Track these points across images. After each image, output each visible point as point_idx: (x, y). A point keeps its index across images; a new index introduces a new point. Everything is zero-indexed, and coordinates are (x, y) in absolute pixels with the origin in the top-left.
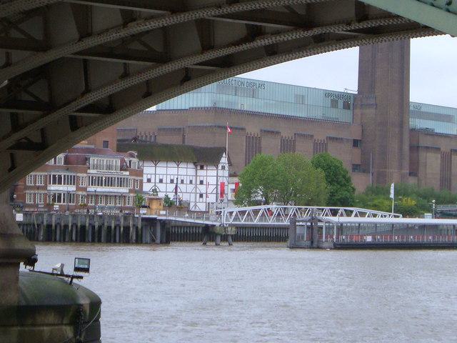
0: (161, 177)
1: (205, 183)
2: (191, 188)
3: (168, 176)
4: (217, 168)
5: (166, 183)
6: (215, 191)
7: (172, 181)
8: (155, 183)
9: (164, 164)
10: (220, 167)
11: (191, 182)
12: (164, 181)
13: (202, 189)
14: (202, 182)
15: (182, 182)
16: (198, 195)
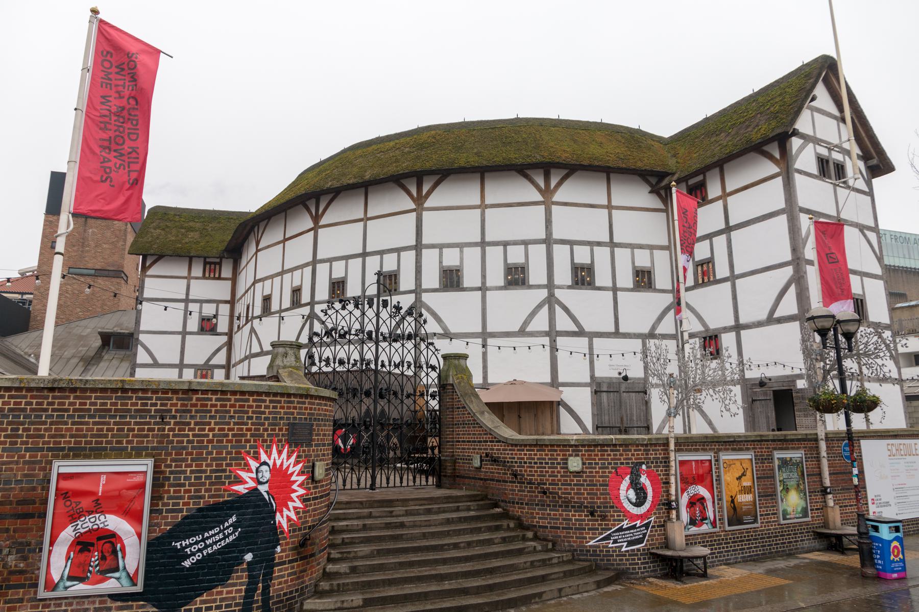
0: (451, 258)
1: (722, 270)
2: (640, 310)
3: (495, 255)
4: (785, 160)
5: (483, 289)
6: (789, 305)
7: (516, 277)
8: (418, 291)
9: (464, 193)
10: (805, 159)
11: (644, 279)
12: (471, 278)
13: (712, 306)
14: (705, 274)
15: (583, 277)
16: (693, 347)
